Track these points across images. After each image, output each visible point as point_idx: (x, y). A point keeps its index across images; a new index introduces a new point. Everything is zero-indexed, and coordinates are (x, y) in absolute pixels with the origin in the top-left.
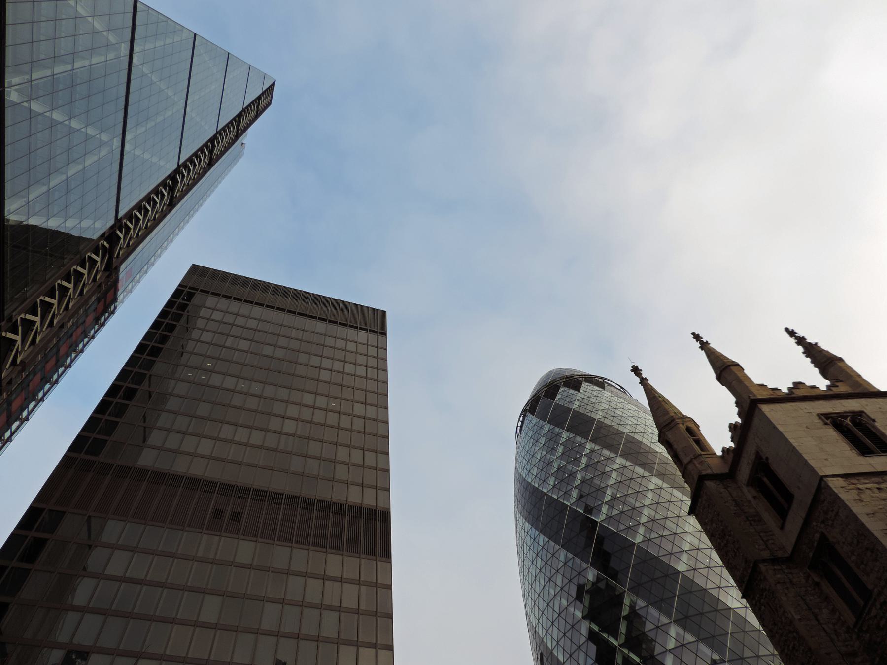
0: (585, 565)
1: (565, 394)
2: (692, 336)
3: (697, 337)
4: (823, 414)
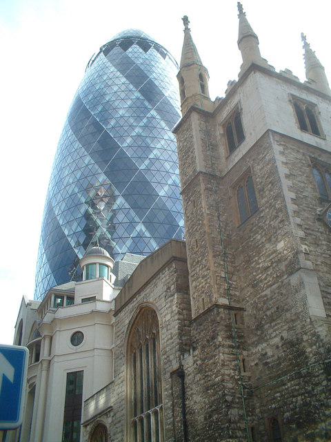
0: (100, 171)
1: (136, 50)
2: (237, 4)
3: (240, 6)
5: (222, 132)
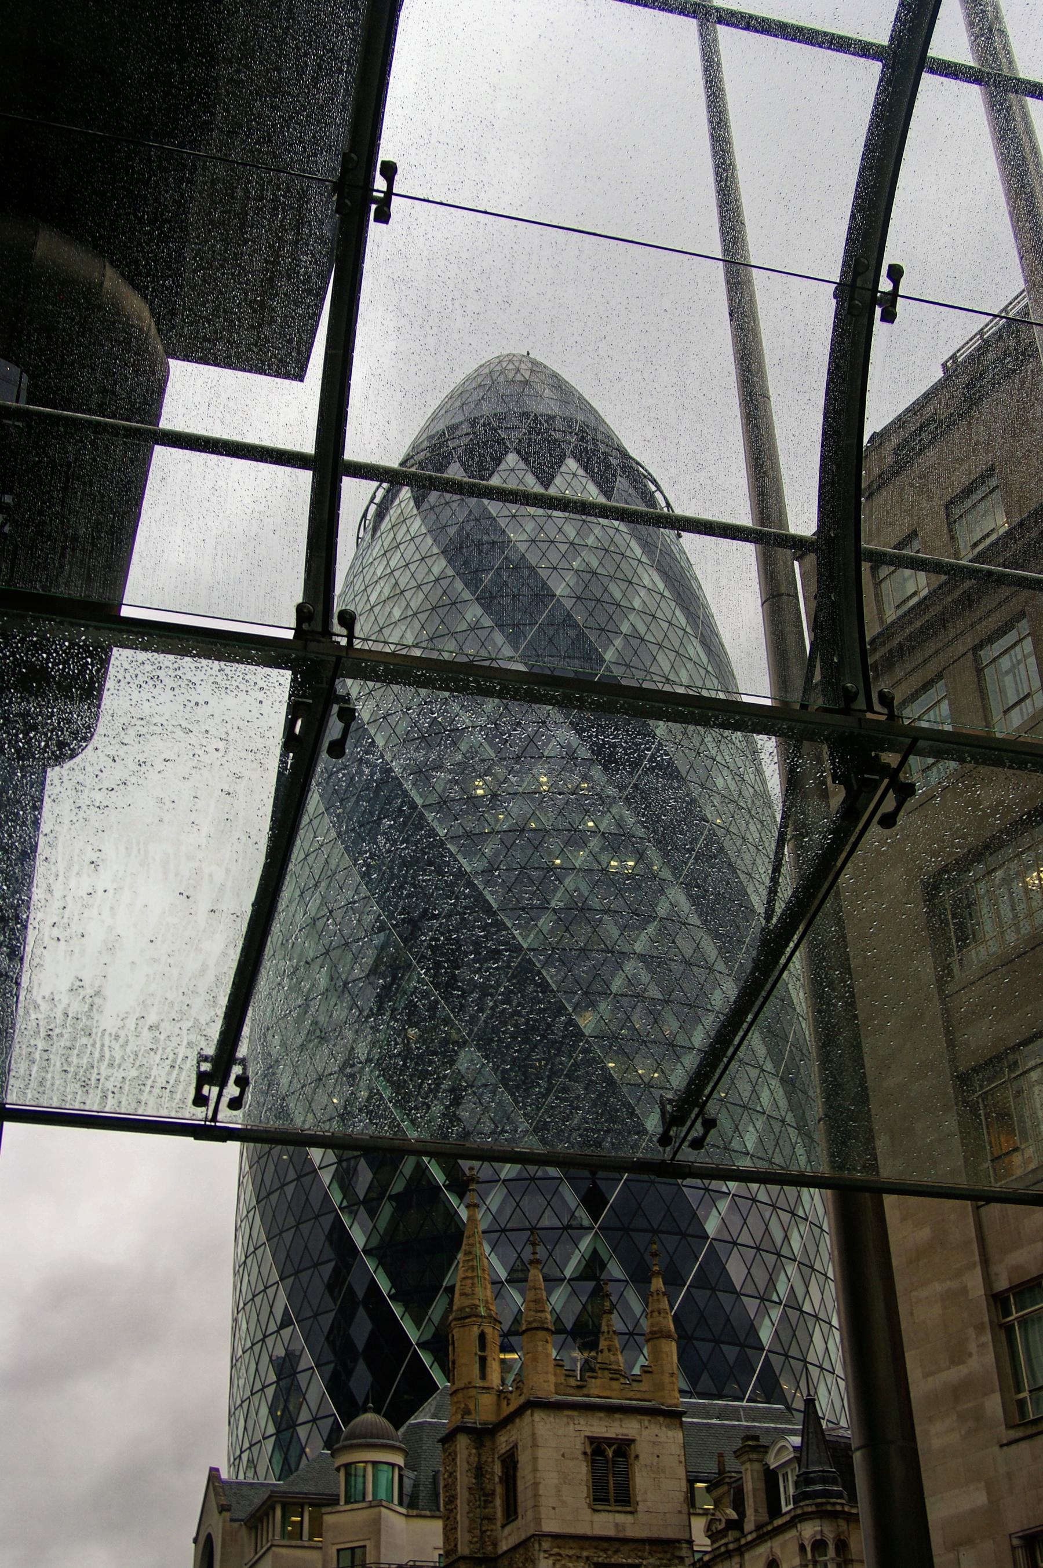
4: (589, 1438)
5: (500, 1474)
